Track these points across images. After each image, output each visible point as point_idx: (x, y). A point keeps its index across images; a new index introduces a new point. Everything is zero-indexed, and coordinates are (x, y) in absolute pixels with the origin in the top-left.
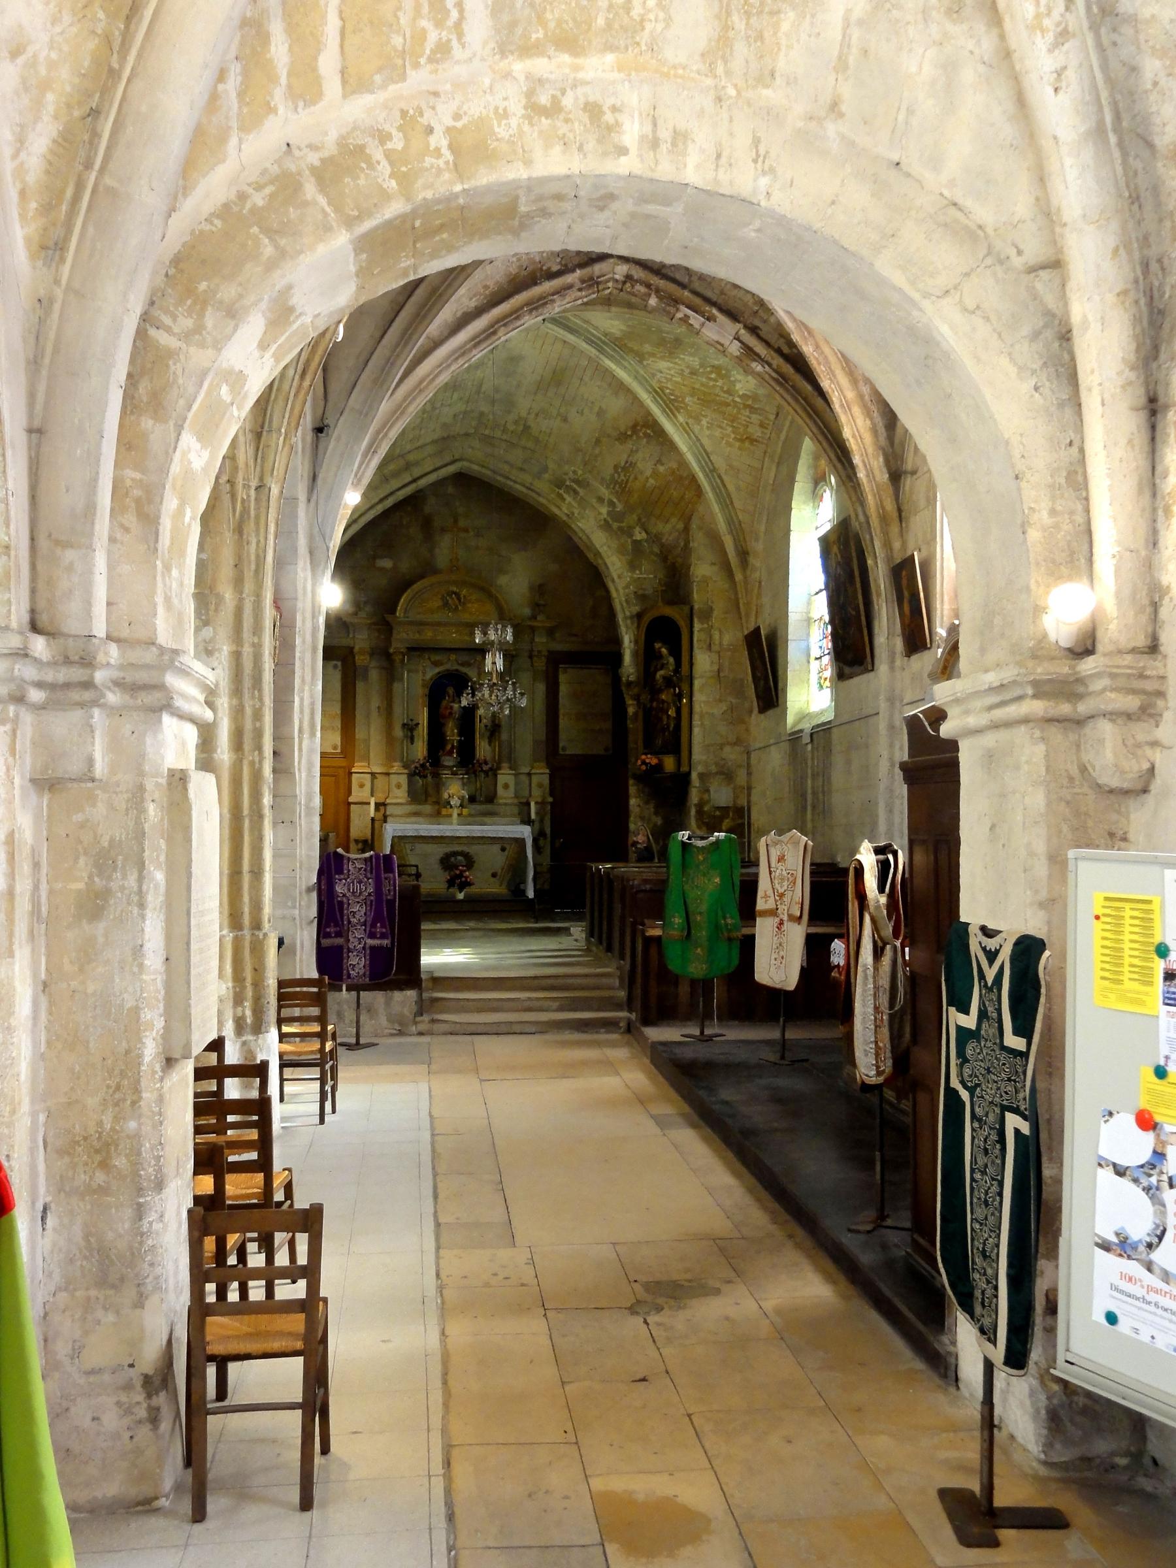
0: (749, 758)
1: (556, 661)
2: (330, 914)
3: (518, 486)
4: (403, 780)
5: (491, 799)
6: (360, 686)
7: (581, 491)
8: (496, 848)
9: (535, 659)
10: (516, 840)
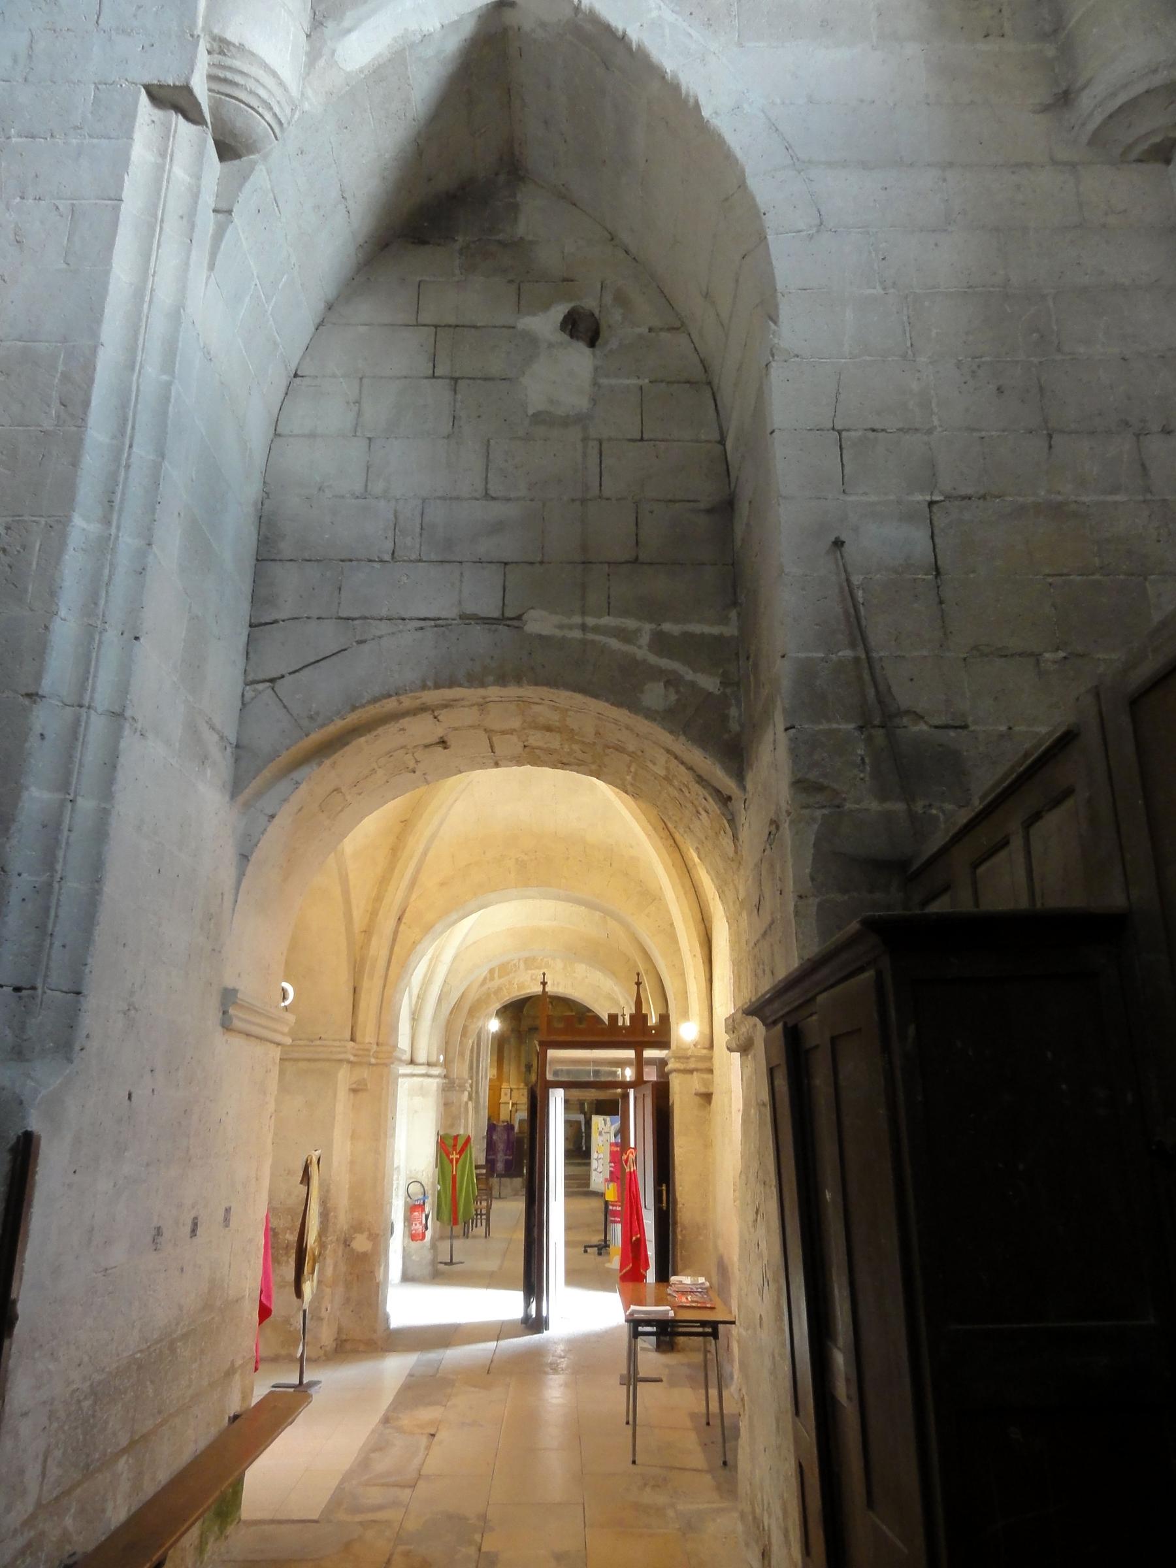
2: (491, 1147)
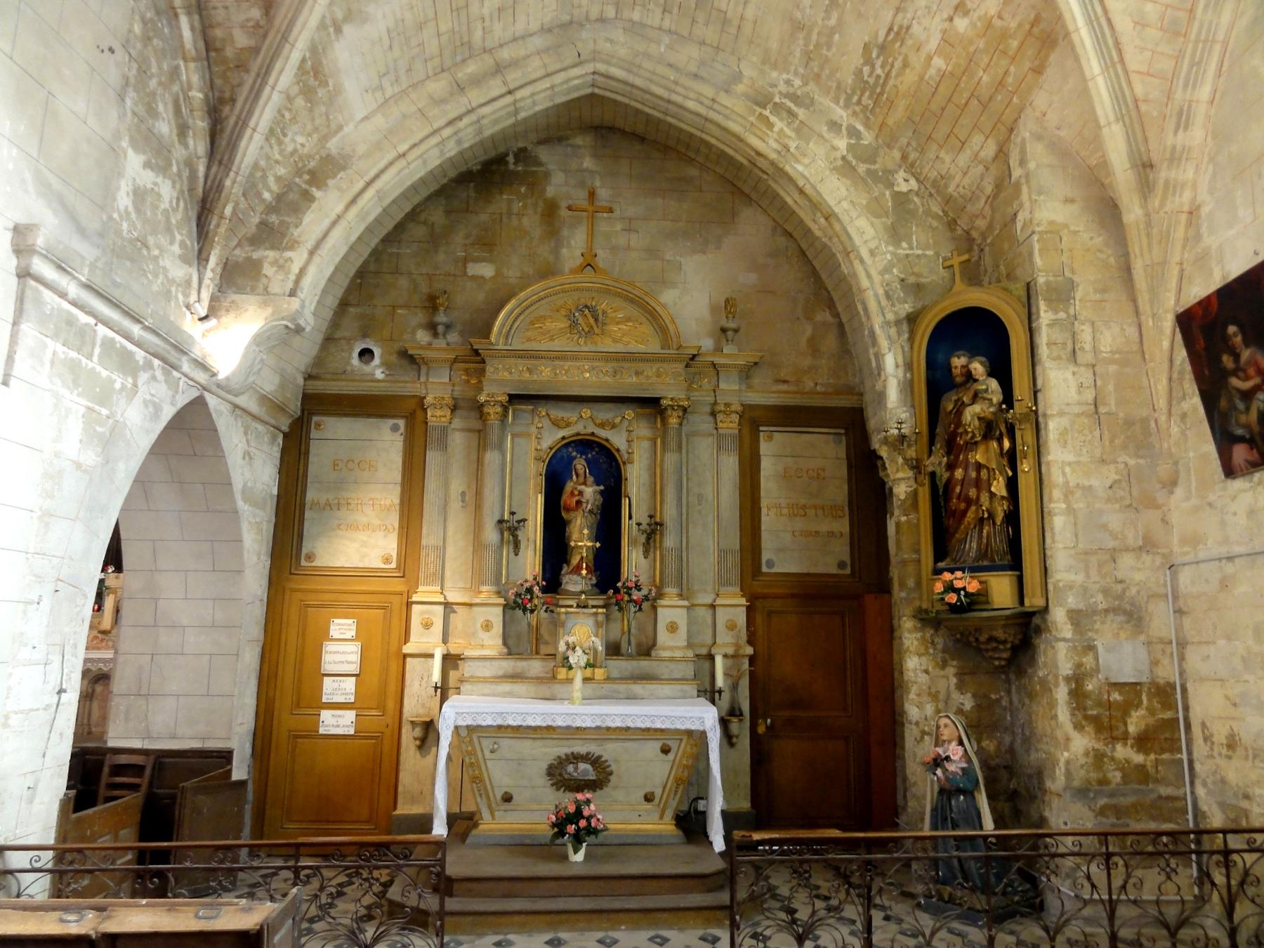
0: (1174, 579)
1: (755, 421)
3: (691, 105)
4: (495, 615)
5: (646, 650)
6: (433, 458)
7: (801, 113)
8: (653, 748)
9: (720, 417)
10: (689, 733)
